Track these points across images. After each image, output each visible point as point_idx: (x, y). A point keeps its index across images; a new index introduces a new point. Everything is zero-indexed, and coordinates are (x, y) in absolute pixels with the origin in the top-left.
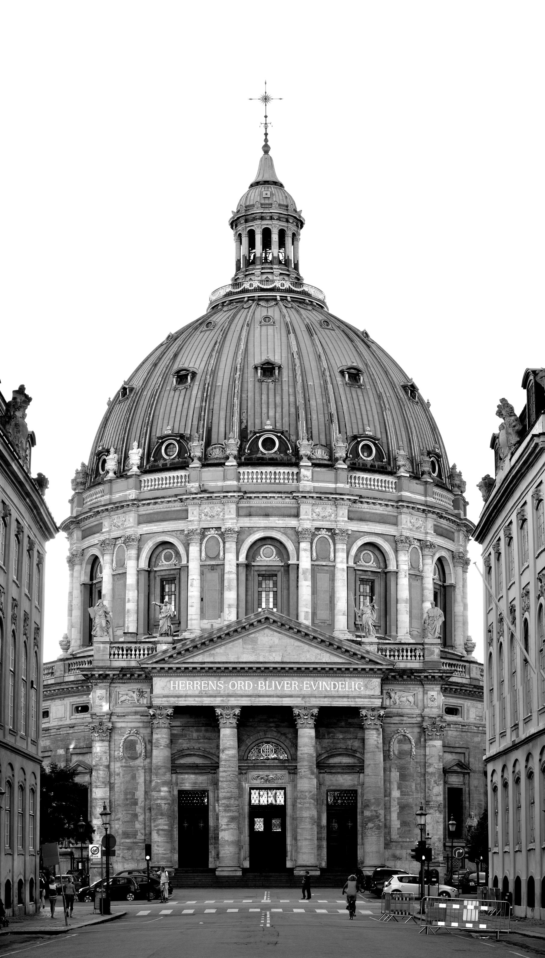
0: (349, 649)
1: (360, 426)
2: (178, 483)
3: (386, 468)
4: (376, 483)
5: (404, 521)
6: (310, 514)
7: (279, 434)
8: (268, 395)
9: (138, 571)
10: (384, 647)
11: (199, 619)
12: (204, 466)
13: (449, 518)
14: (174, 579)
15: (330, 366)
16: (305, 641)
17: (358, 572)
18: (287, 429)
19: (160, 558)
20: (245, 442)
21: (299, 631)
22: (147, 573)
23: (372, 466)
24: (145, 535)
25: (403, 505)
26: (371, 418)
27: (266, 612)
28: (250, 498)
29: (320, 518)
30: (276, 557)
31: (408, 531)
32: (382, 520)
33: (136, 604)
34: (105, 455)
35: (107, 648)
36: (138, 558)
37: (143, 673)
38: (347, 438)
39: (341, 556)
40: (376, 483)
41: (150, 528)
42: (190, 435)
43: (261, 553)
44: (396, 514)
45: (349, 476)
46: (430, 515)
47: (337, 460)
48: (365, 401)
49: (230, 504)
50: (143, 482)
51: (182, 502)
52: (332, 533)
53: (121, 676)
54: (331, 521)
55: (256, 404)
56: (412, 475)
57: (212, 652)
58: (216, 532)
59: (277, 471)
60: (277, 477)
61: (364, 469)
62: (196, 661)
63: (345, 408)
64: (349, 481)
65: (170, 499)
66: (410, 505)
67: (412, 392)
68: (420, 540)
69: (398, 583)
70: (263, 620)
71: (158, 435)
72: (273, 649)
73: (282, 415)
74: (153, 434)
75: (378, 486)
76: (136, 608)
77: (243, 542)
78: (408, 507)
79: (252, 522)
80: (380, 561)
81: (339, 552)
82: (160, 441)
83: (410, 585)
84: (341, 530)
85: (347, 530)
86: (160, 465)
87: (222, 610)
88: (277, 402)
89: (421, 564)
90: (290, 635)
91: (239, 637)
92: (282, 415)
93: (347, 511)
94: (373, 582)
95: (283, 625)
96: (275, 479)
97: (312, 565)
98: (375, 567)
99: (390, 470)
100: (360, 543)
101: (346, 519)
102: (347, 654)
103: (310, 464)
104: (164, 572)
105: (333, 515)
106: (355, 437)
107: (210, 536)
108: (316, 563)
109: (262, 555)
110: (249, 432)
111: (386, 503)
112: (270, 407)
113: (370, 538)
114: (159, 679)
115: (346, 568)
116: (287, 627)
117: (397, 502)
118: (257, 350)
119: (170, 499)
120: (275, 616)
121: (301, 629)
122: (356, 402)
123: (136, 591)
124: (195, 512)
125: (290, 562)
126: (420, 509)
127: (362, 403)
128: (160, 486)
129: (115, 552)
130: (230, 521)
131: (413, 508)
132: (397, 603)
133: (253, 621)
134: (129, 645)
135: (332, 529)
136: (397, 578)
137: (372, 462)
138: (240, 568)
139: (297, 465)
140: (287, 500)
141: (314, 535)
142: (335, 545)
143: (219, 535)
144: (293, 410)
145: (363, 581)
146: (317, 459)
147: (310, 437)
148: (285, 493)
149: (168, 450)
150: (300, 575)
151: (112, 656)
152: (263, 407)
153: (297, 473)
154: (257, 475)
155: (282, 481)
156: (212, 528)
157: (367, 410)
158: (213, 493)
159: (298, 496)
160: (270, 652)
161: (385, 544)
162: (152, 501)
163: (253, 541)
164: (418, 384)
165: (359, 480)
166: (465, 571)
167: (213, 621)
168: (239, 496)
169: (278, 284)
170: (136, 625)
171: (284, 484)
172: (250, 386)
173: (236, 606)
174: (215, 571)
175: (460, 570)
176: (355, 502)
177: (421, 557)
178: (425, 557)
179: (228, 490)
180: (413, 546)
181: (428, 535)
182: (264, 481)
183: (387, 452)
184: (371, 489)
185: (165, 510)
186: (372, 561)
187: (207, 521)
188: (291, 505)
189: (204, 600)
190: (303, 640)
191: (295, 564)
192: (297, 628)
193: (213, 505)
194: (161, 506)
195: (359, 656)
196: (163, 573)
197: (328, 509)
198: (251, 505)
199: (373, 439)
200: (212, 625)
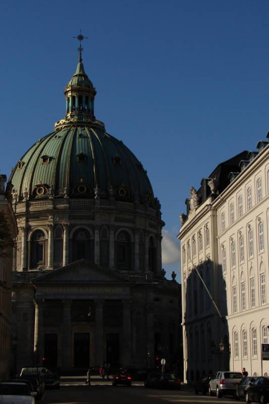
39: (112, 236)
67: (141, 168)
74: (33, 186)
97: (100, 240)
100: (119, 230)
125: (91, 238)
142: (109, 231)
164: (143, 164)
166: (160, 241)
169: (84, 120)
175: (159, 241)
176: (117, 213)
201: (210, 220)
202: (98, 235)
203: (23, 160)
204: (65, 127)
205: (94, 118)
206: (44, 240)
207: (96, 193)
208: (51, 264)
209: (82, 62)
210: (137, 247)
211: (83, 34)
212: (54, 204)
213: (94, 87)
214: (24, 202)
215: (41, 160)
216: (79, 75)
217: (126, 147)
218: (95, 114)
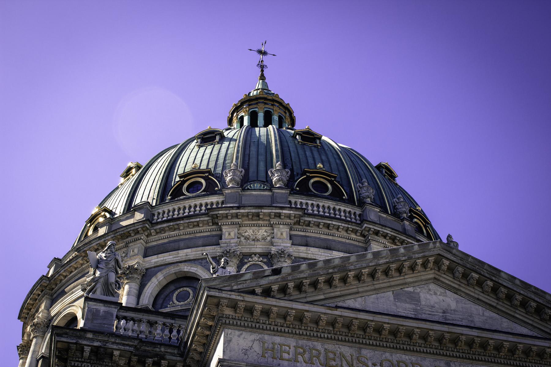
7: (333, 179)
24: (153, 269)
28: (308, 224)
37: (179, 358)
41: (162, 259)
49: (281, 226)
53: (134, 359)
58: (261, 259)
114: (237, 333)
124: (232, 234)
134: (153, 318)
140: (353, 236)
143: (264, 263)
144: (341, 168)
156: (255, 254)
185: (187, 237)
188: (357, 243)
190: (498, 307)
192: (494, 278)
194: (181, 232)
198: (307, 234)
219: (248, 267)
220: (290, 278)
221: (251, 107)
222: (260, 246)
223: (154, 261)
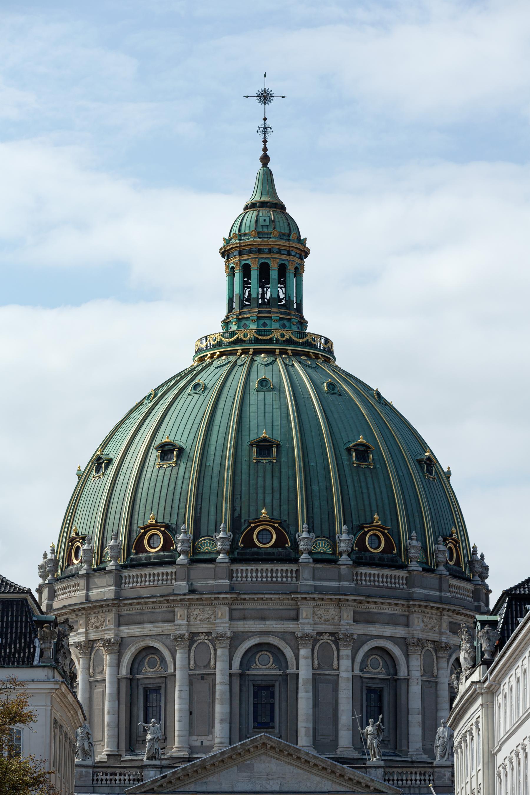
0: (352, 777)
1: (368, 514)
2: (163, 580)
3: (397, 561)
4: (385, 580)
5: (416, 621)
6: (312, 618)
7: (276, 525)
8: (264, 478)
9: (119, 679)
10: (391, 770)
11: (188, 735)
12: (193, 561)
13: (467, 615)
14: (160, 688)
15: (335, 442)
16: (305, 768)
17: (364, 680)
18: (285, 518)
19: (144, 664)
20: (238, 534)
21: (299, 758)
22: (129, 681)
23: (381, 559)
24: (127, 639)
25: (415, 605)
26: (380, 504)
27: (263, 737)
28: (245, 599)
29: (322, 621)
30: (274, 665)
31: (420, 633)
32: (392, 621)
33: (117, 716)
34: (79, 541)
35: (90, 773)
36: (119, 664)
38: (352, 528)
39: (345, 663)
40: (385, 580)
41: (132, 631)
42: (177, 525)
43: (257, 660)
44: (406, 613)
45: (355, 573)
46: (445, 612)
47: (341, 554)
48: (373, 483)
49: (222, 606)
50: (124, 579)
51: (168, 603)
52: (335, 638)
54: (334, 625)
55: (251, 488)
56: (426, 566)
57: (205, 780)
58: (207, 637)
59: (275, 569)
60: (274, 575)
61: (373, 562)
62: (188, 790)
63: (351, 492)
64: (355, 578)
65: (155, 600)
66: (422, 603)
68: (434, 642)
69: (409, 692)
70: (260, 746)
71: (141, 524)
72: (270, 777)
73: (280, 502)
75: (387, 582)
76: (117, 721)
77: (236, 649)
78: (420, 606)
79: (246, 626)
80: (390, 666)
81: (343, 658)
82: (143, 531)
83: (423, 693)
84: (344, 634)
85: (352, 635)
86: (143, 559)
87: (213, 726)
88: (275, 486)
89: (435, 668)
90: (289, 761)
91: (233, 763)
92: (280, 502)
93: (352, 612)
94: (381, 690)
95: (280, 750)
96: (272, 577)
97: (313, 674)
98: (384, 674)
99: (400, 563)
100: (366, 648)
101: (351, 622)
102: (351, 783)
103: (311, 561)
104: (148, 680)
105: (337, 618)
106: (361, 527)
107: (199, 641)
108: (317, 672)
109: (257, 662)
110: (242, 521)
111: (396, 602)
112: (267, 492)
113: (378, 642)
115: (351, 677)
116: (286, 753)
117: (408, 599)
118: (253, 423)
119: (155, 600)
120: (273, 742)
121: (300, 756)
122: (363, 485)
123: (117, 702)
125: (288, 671)
126: (434, 607)
127: (371, 486)
128: (143, 584)
129: (92, 656)
130: (222, 625)
131: (426, 607)
132: (408, 714)
133: (249, 747)
134: (113, 770)
135: (335, 633)
136: (408, 686)
137: (380, 554)
138: (233, 678)
139: (296, 561)
141: (316, 641)
142: (338, 651)
145: (370, 691)
146: (320, 553)
147: (311, 527)
148: (282, 594)
149: (152, 541)
150: (300, 685)
151: (95, 782)
152: (259, 492)
153: (297, 570)
154: (252, 573)
155: (279, 580)
156: (202, 633)
157: (375, 494)
158: (202, 594)
159: (298, 598)
160: (268, 779)
161: (394, 648)
162: (135, 601)
163: (247, 648)
165: (365, 577)
167: (203, 737)
168: (231, 598)
170: (116, 739)
171: (282, 582)
172: (245, 466)
173: (228, 721)
174: (205, 681)
176: (361, 602)
177: (435, 660)
178: (440, 660)
179: (221, 591)
180: (427, 648)
181: (443, 636)
182: (259, 579)
183: (397, 542)
184: (379, 586)
186: (381, 667)
187: (197, 625)
189: (193, 713)
190: (302, 767)
191: (295, 674)
193: (202, 607)
194: (145, 606)
195: (363, 785)
196: (147, 682)
197: (332, 611)
198: (245, 607)
199: (381, 528)
200: (202, 742)
201: (480, 714)
202: (310, 661)
203: (105, 452)
204: (222, 354)
205: (303, 323)
206: (163, 675)
207: (302, 546)
208: (179, 742)
209: (269, 165)
210: (415, 689)
211: (270, 87)
212: (188, 578)
213: (302, 238)
214: (110, 572)
215: (154, 455)
216: (263, 205)
217: (395, 408)
218: (306, 314)
219: (197, 645)
220: (172, 778)
221: (243, 257)
222: (206, 626)
223: (126, 631)
